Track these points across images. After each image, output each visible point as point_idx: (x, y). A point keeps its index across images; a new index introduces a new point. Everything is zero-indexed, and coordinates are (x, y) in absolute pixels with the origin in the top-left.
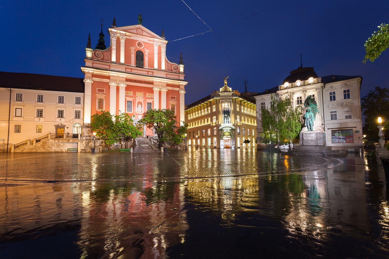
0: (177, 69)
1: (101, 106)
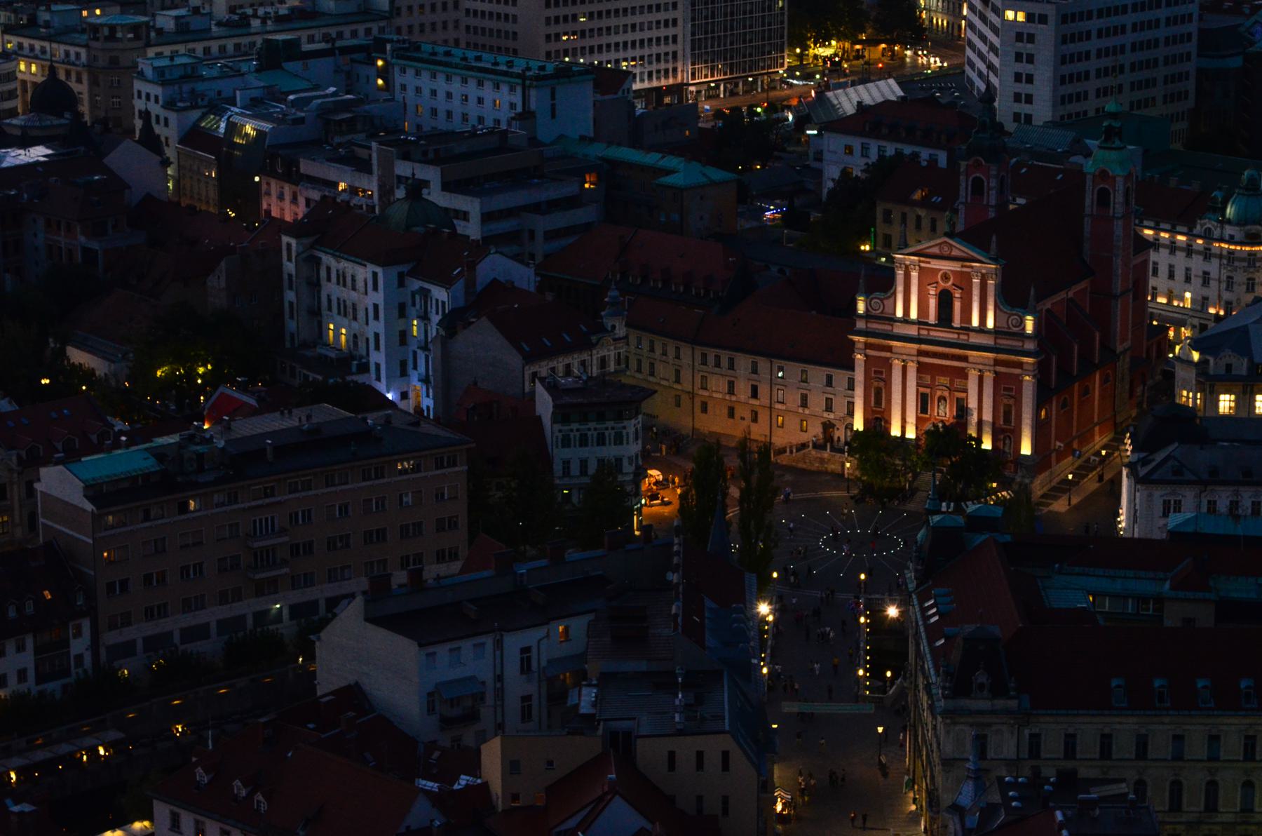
0: (1022, 323)
1: (878, 402)
